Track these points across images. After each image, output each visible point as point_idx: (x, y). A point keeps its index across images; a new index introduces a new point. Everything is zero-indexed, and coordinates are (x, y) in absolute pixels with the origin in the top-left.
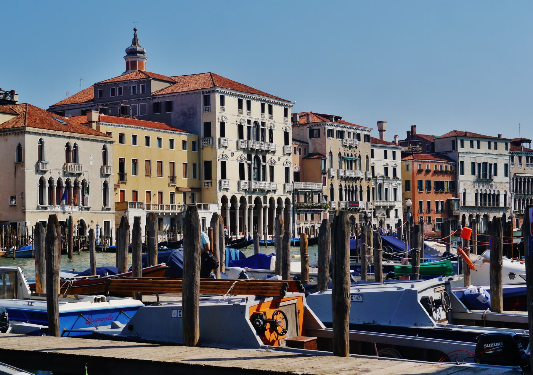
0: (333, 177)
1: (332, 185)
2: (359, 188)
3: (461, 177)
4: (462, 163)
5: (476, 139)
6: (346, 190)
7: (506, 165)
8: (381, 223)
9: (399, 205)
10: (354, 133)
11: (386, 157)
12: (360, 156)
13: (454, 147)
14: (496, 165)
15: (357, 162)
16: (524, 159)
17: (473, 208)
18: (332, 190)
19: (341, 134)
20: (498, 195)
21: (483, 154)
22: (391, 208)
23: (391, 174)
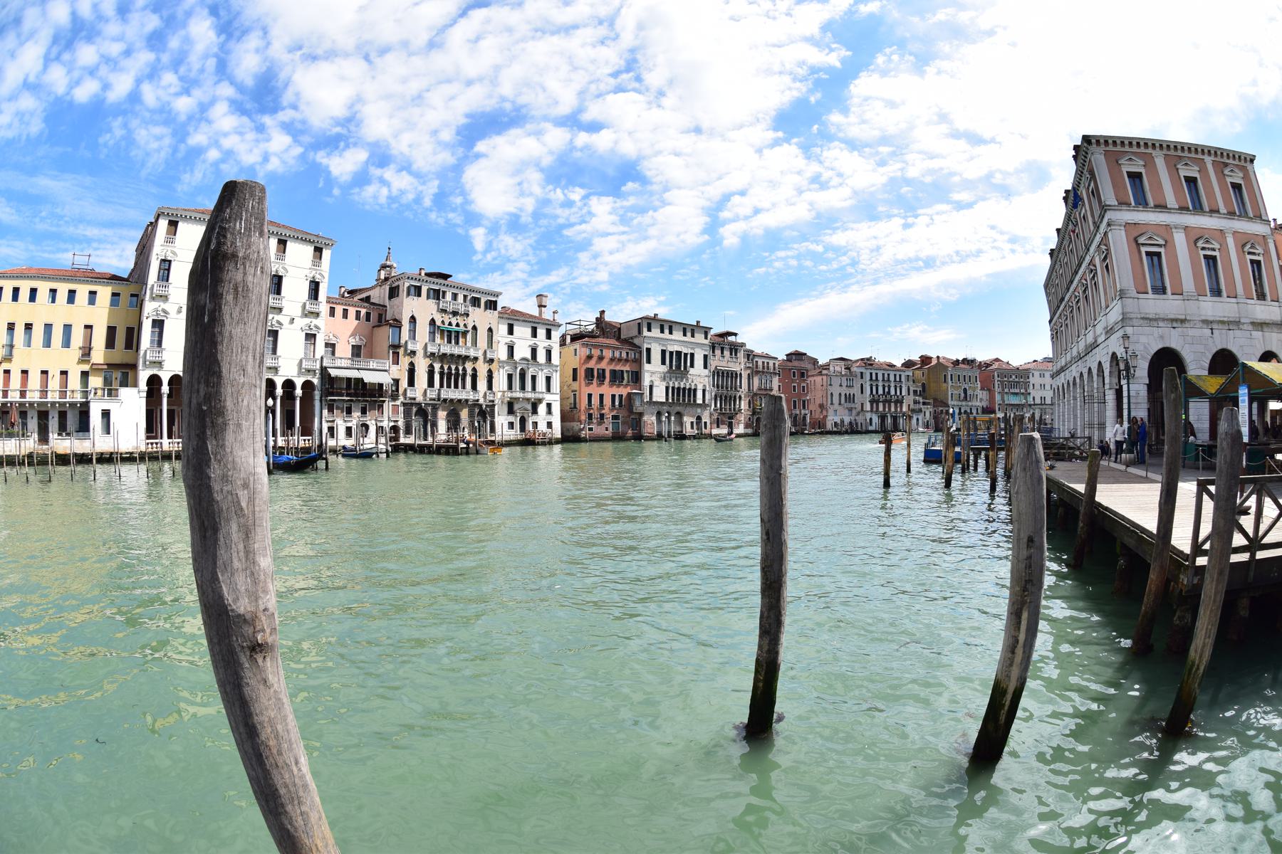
0: (413, 353)
1: (412, 364)
2: (469, 372)
3: (647, 367)
4: (649, 350)
5: (668, 326)
6: (442, 374)
7: (705, 357)
8: (523, 421)
9: (554, 399)
10: (465, 297)
11: (534, 335)
12: (475, 328)
13: (640, 332)
14: (692, 355)
15: (469, 336)
16: (727, 353)
17: (662, 403)
18: (412, 372)
19: (437, 295)
20: (695, 390)
21: (677, 341)
22: (540, 401)
23: (541, 357)
